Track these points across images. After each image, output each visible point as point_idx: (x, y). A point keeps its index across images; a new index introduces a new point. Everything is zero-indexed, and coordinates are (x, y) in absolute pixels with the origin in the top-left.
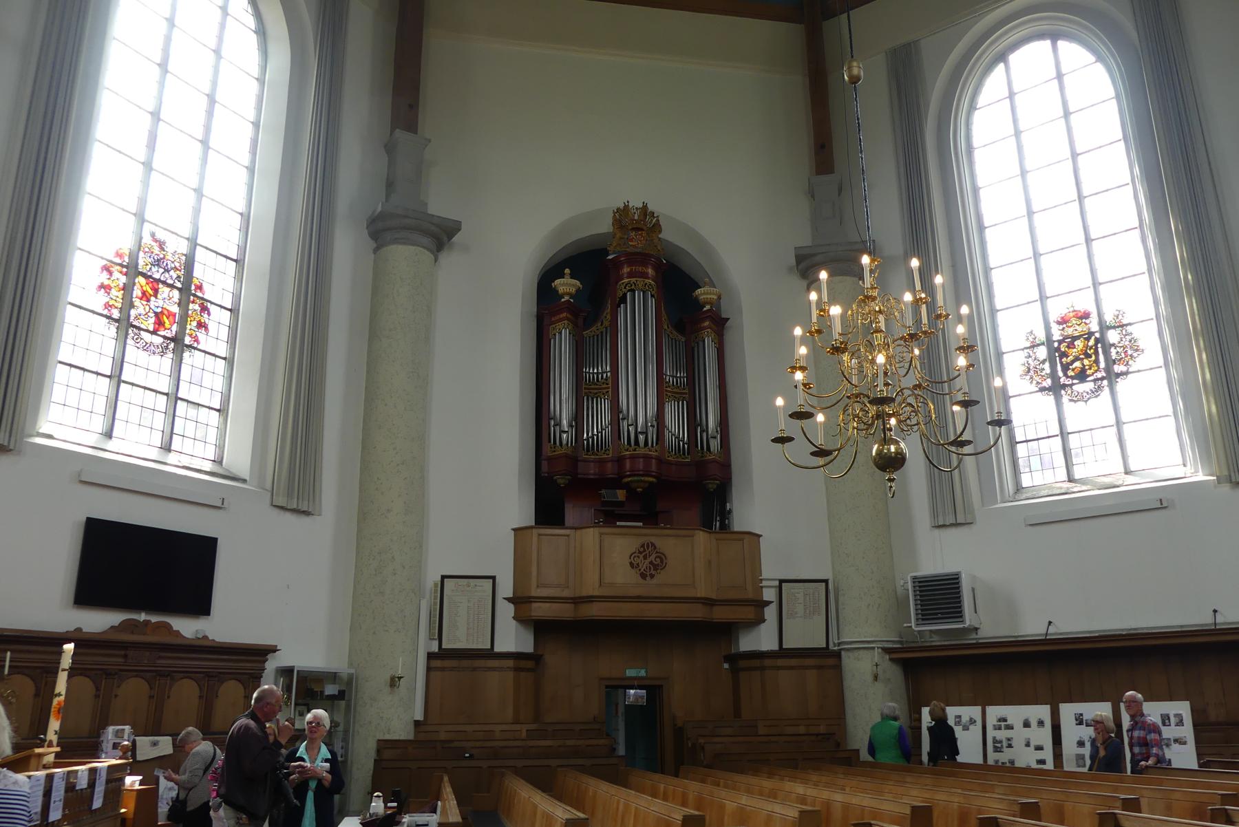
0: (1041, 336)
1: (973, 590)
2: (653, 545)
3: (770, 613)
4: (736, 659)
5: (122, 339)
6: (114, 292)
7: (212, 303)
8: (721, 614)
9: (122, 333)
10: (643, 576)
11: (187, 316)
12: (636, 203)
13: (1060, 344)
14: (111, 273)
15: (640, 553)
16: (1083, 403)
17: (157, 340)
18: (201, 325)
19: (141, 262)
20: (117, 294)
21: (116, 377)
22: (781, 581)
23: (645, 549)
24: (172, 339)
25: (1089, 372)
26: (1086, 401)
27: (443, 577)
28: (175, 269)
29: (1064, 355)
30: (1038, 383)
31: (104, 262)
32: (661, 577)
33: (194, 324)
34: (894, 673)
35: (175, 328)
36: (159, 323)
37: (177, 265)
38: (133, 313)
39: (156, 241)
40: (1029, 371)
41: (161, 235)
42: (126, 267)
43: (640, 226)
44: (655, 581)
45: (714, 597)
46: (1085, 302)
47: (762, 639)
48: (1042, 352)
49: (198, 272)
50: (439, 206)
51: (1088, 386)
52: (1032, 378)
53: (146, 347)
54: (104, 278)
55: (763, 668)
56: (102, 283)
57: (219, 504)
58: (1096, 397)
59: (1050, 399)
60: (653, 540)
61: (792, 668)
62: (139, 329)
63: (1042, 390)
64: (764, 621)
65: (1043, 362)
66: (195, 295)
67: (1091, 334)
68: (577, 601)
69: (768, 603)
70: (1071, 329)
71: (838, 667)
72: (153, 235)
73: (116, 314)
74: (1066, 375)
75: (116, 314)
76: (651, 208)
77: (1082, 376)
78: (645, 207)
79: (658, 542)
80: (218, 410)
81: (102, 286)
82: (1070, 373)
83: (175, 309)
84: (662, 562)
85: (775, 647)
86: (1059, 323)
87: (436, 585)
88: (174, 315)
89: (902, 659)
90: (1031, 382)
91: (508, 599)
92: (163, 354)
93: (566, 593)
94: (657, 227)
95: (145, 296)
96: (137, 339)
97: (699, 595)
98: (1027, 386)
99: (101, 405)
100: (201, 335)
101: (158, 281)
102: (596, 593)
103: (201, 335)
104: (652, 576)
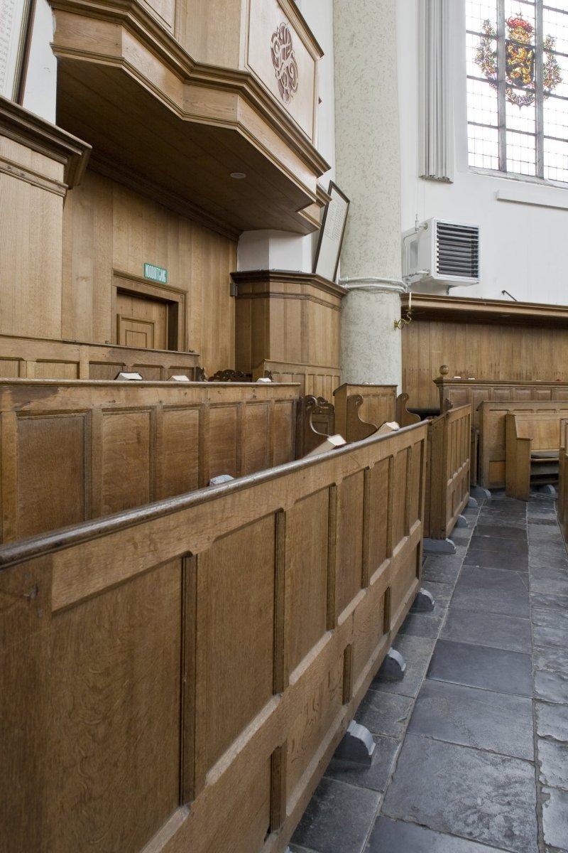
0: (495, 27)
16: (517, 107)
25: (525, 81)
26: (520, 106)
40: (482, 58)
51: (520, 93)
52: (483, 65)
58: (528, 105)
63: (490, 81)
65: (495, 54)
70: (517, 36)
74: (509, 75)
77: (519, 83)
90: (483, 70)
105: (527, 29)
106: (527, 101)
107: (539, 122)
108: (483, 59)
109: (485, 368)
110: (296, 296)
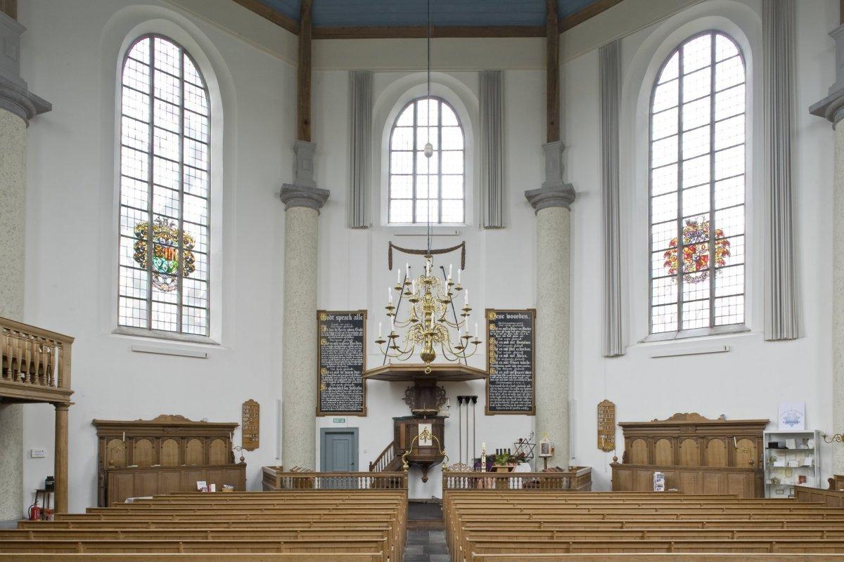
6: (673, 263)
17: (699, 274)
18: (726, 253)
19: (684, 240)
20: (675, 263)
24: (708, 269)
31: (664, 253)
35: (708, 263)
41: (692, 220)
49: (718, 226)
53: (695, 281)
54: (667, 259)
57: (724, 350)
72: (688, 223)
73: (675, 272)
83: (707, 253)
88: (705, 257)
95: (689, 256)
96: (688, 279)
100: (726, 259)
101: (696, 243)
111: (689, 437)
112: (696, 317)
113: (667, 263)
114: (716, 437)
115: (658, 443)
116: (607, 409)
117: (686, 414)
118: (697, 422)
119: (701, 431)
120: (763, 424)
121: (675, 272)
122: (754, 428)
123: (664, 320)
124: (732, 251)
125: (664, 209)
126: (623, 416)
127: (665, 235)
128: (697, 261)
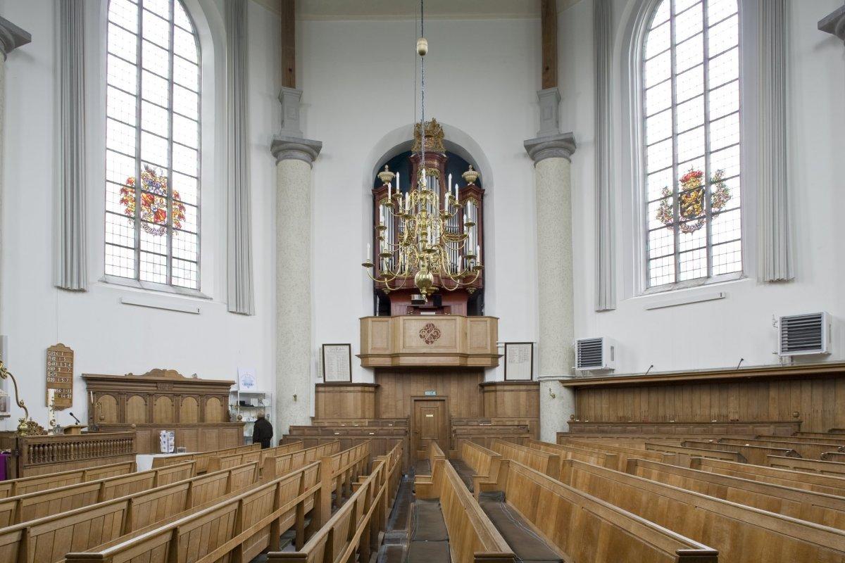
0: (671, 189)
1: (612, 348)
2: (433, 325)
3: (501, 361)
4: (483, 386)
5: (137, 228)
6: (130, 203)
7: (185, 203)
8: (471, 362)
9: (137, 225)
10: (427, 342)
11: (172, 212)
12: (428, 119)
13: (681, 195)
14: (126, 193)
15: (425, 329)
17: (157, 227)
19: (142, 184)
21: (137, 249)
22: (506, 344)
23: (429, 327)
26: (692, 232)
27: (323, 345)
28: (162, 187)
29: (683, 202)
30: (666, 221)
32: (437, 342)
33: (177, 216)
34: (567, 395)
35: (166, 220)
36: (157, 217)
37: (163, 184)
38: (142, 214)
39: (149, 172)
41: (151, 167)
42: (135, 188)
43: (429, 134)
44: (433, 345)
45: (468, 353)
46: (699, 166)
47: (495, 376)
48: (670, 201)
50: (312, 133)
51: (695, 222)
53: (152, 232)
55: (495, 391)
56: (123, 199)
58: (699, 229)
59: (671, 232)
60: (433, 322)
61: (512, 391)
62: (147, 222)
63: (668, 226)
64: (498, 365)
66: (175, 200)
67: (701, 187)
68: (394, 356)
69: (501, 356)
71: (538, 390)
72: (147, 168)
74: (682, 213)
75: (133, 215)
76: (438, 121)
77: (691, 217)
78: (434, 121)
79: (436, 324)
80: (196, 263)
81: (123, 201)
82: (686, 214)
84: (438, 334)
85: (503, 380)
86: (683, 181)
87: (320, 349)
89: (572, 386)
91: (358, 356)
92: (161, 235)
93: (387, 352)
94: (441, 134)
96: (146, 228)
97: (458, 352)
98: (659, 223)
99: (132, 264)
100: (182, 222)
101: (154, 194)
102: (401, 352)
103: (182, 222)
104: (432, 342)
105: (698, 175)
106: (698, 227)
107: (709, 236)
108: (662, 214)
109: (638, 414)
110: (493, 391)
111: (165, 395)
112: (153, 272)
113: (123, 201)
114: (190, 394)
115: (130, 400)
116: (60, 359)
117: (164, 371)
118: (175, 380)
119: (177, 389)
120: (228, 385)
121: (133, 215)
122: (220, 389)
123: (118, 263)
124: (186, 216)
125: (118, 137)
126: (83, 366)
127: (120, 169)
128: (155, 213)
